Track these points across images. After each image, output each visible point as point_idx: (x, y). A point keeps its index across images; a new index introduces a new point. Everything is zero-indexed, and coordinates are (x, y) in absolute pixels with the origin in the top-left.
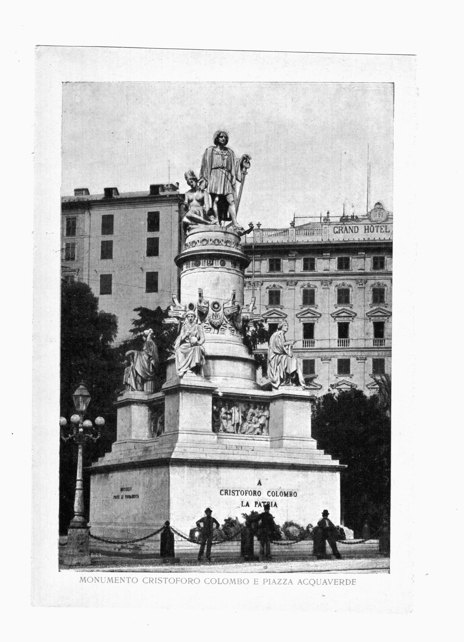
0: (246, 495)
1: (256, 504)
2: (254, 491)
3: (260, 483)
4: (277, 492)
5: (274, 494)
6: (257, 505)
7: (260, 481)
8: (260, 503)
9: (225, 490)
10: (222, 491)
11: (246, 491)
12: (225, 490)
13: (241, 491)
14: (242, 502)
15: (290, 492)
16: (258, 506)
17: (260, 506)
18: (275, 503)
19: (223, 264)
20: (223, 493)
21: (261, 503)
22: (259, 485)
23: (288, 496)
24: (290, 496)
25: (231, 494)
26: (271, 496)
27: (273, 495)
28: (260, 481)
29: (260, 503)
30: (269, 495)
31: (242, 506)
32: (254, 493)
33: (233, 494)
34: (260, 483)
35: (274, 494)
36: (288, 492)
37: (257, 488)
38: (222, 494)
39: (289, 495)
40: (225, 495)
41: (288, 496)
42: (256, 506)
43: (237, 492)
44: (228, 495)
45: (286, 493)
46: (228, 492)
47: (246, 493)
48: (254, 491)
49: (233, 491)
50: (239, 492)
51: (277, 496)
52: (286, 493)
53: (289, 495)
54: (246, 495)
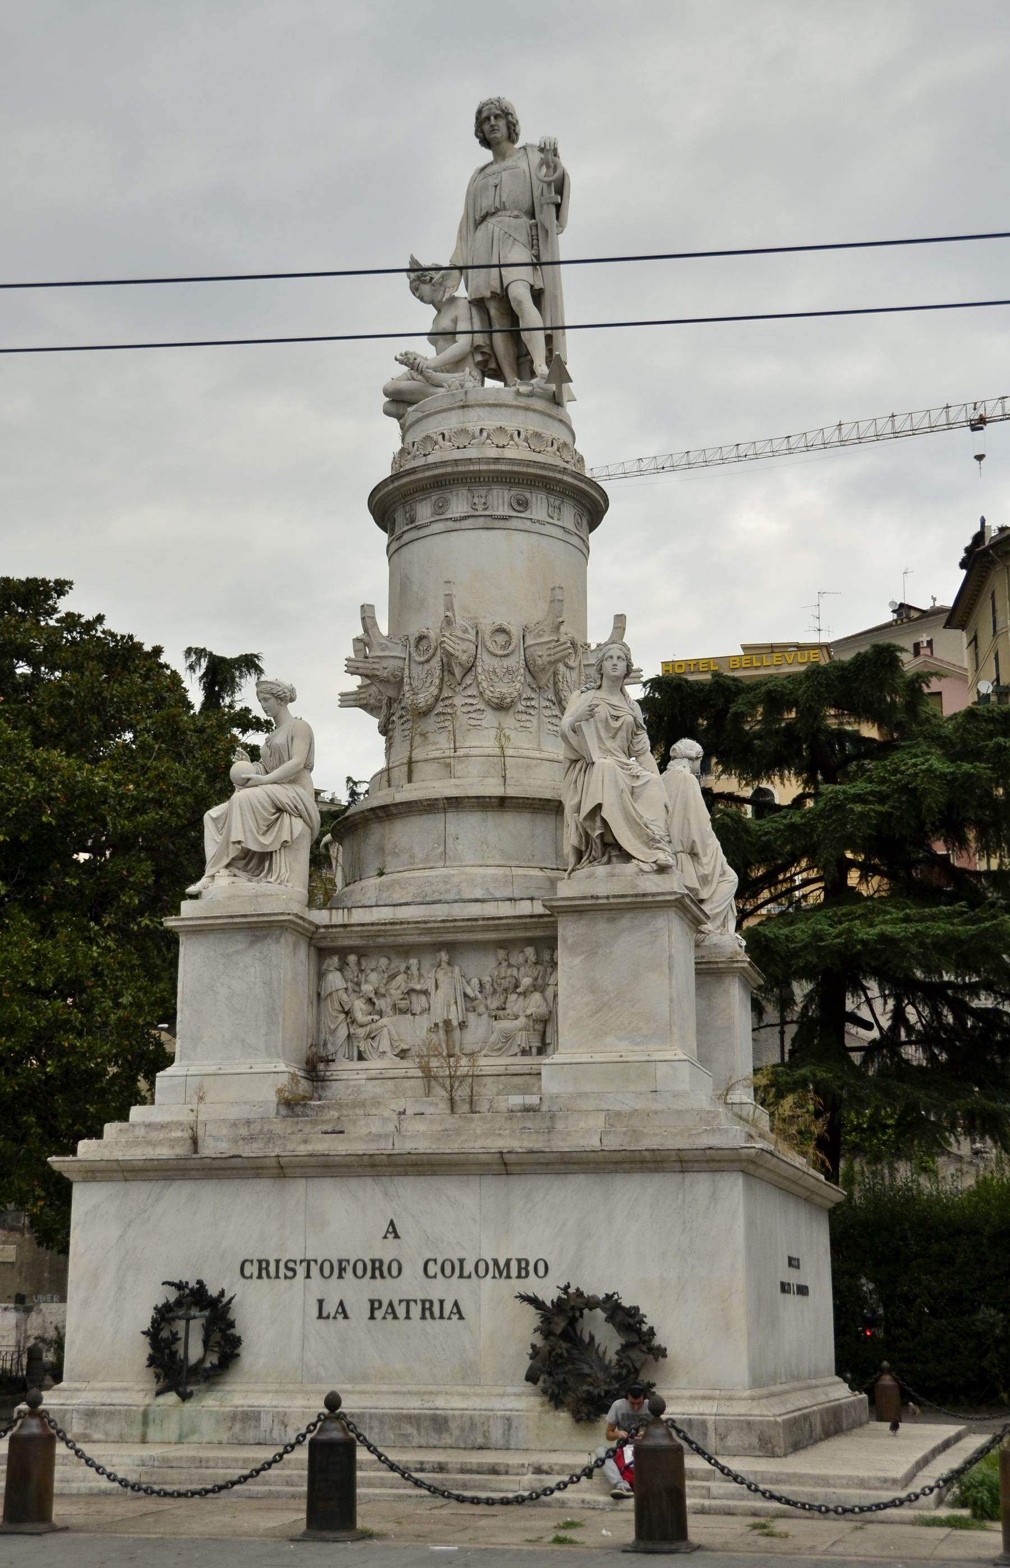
0: (340, 1277)
1: (373, 1310)
2: (373, 1261)
3: (393, 1230)
4: (461, 1261)
5: (455, 1269)
6: (379, 1314)
7: (392, 1223)
8: (391, 1304)
9: (260, 1262)
10: (247, 1265)
11: (340, 1262)
12: (260, 1262)
13: (319, 1263)
14: (321, 1302)
15: (519, 1261)
16: (384, 1318)
17: (390, 1317)
18: (456, 1304)
19: (440, 509)
20: (251, 1269)
21: (396, 1304)
22: (390, 1236)
23: (508, 1277)
24: (519, 1276)
25: (281, 1275)
26: (439, 1275)
27: (448, 1270)
28: (392, 1223)
29: (391, 1304)
30: (431, 1273)
31: (320, 1316)
32: (374, 1269)
33: (290, 1274)
34: (393, 1230)
35: (455, 1269)
36: (508, 1263)
37: (386, 1250)
38: (247, 1273)
39: (514, 1272)
40: (260, 1277)
41: (508, 1277)
42: (372, 1317)
43: (304, 1264)
44: (268, 1276)
45: (502, 1264)
46: (272, 1269)
47: (342, 1270)
48: (373, 1261)
49: (291, 1265)
50: (315, 1269)
51: (461, 1276)
52: (502, 1264)
53: (514, 1272)
54: (340, 1277)
